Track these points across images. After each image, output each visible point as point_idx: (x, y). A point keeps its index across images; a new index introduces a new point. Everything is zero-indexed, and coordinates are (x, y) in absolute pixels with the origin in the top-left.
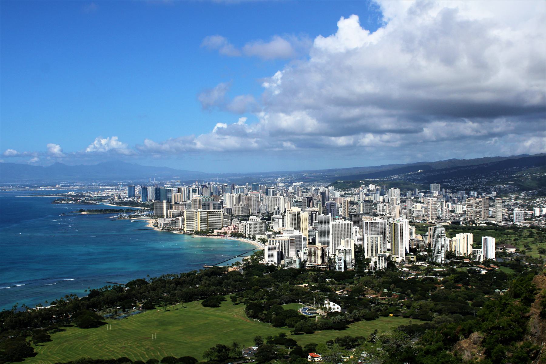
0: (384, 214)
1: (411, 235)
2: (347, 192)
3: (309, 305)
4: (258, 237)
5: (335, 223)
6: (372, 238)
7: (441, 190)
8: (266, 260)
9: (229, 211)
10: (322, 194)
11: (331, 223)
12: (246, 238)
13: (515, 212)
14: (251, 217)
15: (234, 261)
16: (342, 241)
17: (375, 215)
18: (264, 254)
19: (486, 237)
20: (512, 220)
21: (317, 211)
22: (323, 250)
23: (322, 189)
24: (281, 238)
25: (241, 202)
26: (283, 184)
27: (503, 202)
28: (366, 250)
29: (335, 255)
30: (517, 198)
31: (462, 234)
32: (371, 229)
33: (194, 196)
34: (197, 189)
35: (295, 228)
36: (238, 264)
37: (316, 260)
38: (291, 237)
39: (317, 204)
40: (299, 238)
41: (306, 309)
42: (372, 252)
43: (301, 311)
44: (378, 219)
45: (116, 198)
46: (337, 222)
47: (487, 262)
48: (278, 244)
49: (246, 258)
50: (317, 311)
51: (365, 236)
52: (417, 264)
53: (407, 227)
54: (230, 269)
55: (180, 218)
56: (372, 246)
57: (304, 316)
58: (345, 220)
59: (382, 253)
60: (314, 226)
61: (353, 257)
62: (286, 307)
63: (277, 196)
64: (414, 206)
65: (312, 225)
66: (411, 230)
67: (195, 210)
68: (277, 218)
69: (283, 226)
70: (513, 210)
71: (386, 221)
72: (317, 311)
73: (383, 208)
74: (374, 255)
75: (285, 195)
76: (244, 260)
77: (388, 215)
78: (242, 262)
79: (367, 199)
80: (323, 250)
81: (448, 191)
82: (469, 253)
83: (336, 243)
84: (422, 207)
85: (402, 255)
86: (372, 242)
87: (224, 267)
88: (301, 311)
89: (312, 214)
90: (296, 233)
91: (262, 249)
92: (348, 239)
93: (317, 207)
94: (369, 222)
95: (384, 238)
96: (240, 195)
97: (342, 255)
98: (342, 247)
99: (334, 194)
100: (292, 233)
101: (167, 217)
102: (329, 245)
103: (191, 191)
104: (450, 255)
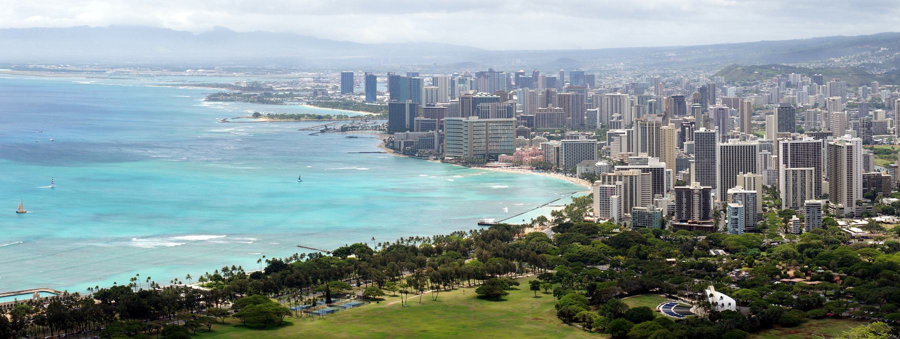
0: (817, 128)
1: (867, 167)
2: (748, 88)
3: (677, 299)
4: (580, 169)
5: (725, 144)
8: (594, 215)
11: (719, 144)
12: (558, 171)
16: (740, 176)
17: (802, 132)
18: (592, 202)
21: (691, 123)
22: (705, 194)
24: (625, 173)
25: (550, 105)
26: (629, 73)
28: (782, 196)
29: (725, 205)
32: (792, 156)
33: (463, 94)
34: (468, 78)
36: (542, 220)
37: (689, 215)
38: (644, 170)
39: (693, 109)
40: (658, 174)
41: (671, 305)
42: (794, 198)
43: (661, 309)
44: (806, 139)
45: (319, 92)
46: (731, 142)
48: (618, 183)
49: (559, 209)
50: (692, 310)
51: (782, 167)
52: (878, 219)
53: (860, 152)
54: (528, 231)
55: (435, 133)
57: (665, 318)
58: (744, 140)
59: (813, 201)
60: (685, 150)
62: (632, 303)
63: (619, 94)
64: (870, 113)
65: (682, 147)
66: (866, 158)
67: (464, 119)
68: (617, 134)
69: (629, 150)
71: (821, 140)
72: (692, 310)
73: (815, 119)
74: (799, 205)
75: (632, 91)
76: (553, 214)
78: (550, 218)
84: (887, 116)
85: (850, 204)
86: (795, 181)
87: (518, 227)
88: (661, 309)
89: (683, 128)
90: (654, 163)
92: (749, 174)
93: (693, 114)
94: (789, 143)
96: (548, 92)
98: (738, 189)
99: (725, 91)
100: (646, 162)
102: (714, 188)
103: (456, 84)
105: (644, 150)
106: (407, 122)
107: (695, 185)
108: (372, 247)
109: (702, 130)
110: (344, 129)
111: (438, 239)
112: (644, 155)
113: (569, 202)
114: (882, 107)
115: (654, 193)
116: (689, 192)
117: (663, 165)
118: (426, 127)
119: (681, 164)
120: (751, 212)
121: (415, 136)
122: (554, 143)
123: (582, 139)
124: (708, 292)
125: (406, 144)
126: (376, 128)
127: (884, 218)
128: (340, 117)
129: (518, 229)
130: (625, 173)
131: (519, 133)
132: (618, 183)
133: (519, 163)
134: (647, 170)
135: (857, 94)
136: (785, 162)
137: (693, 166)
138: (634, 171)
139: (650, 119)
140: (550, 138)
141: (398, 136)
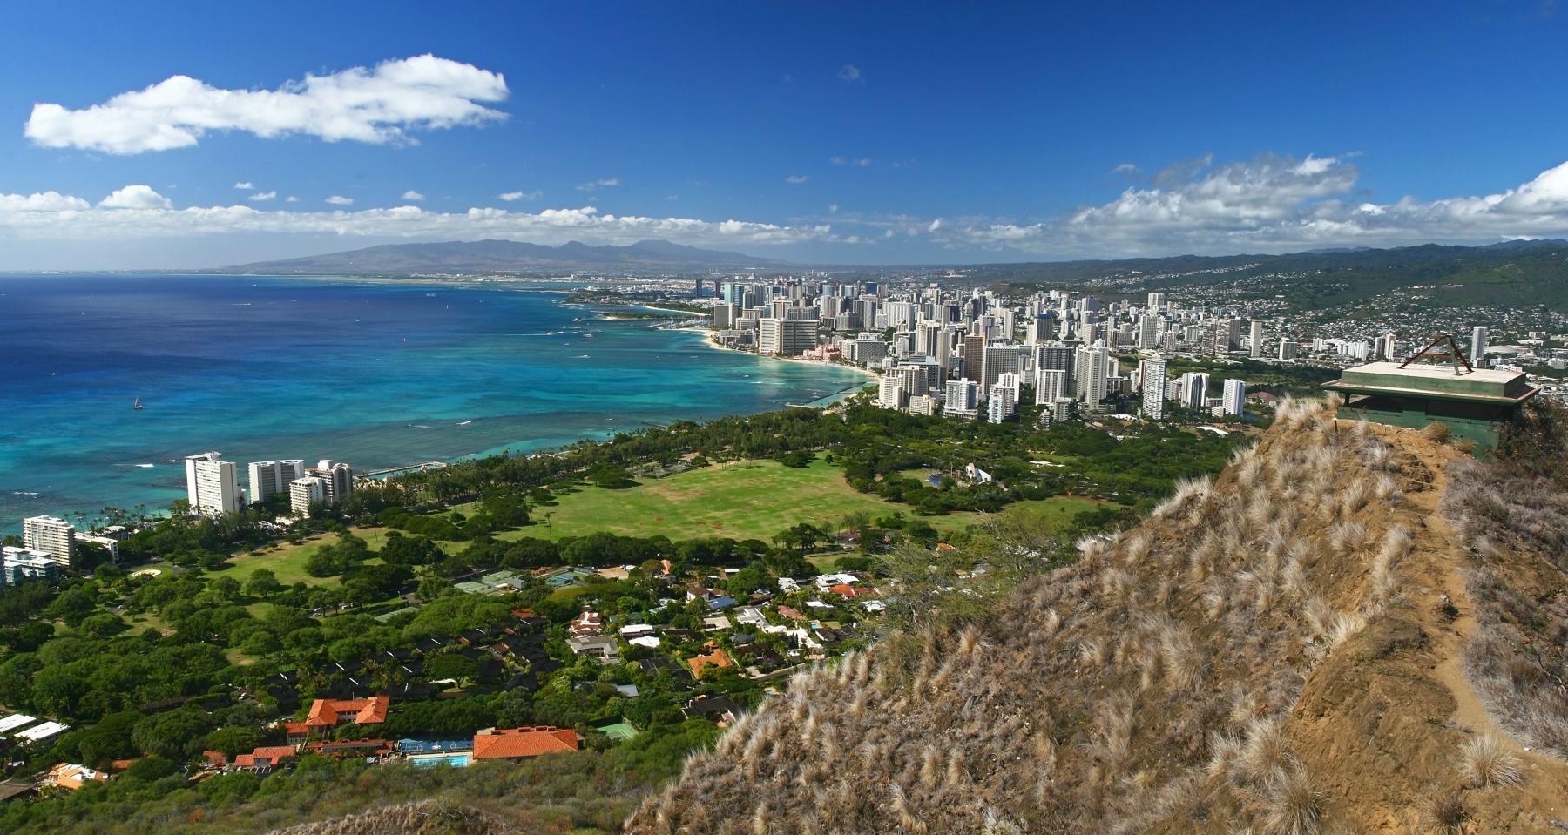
10: (975, 301)
11: (985, 348)
15: (831, 400)
16: (1001, 377)
23: (976, 295)
46: (996, 346)
47: (1227, 419)
54: (826, 412)
61: (1016, 399)
80: (971, 390)
83: (993, 379)
85: (1094, 401)
97: (1000, 398)
109: (972, 335)
123: (873, 338)
136: (1041, 365)
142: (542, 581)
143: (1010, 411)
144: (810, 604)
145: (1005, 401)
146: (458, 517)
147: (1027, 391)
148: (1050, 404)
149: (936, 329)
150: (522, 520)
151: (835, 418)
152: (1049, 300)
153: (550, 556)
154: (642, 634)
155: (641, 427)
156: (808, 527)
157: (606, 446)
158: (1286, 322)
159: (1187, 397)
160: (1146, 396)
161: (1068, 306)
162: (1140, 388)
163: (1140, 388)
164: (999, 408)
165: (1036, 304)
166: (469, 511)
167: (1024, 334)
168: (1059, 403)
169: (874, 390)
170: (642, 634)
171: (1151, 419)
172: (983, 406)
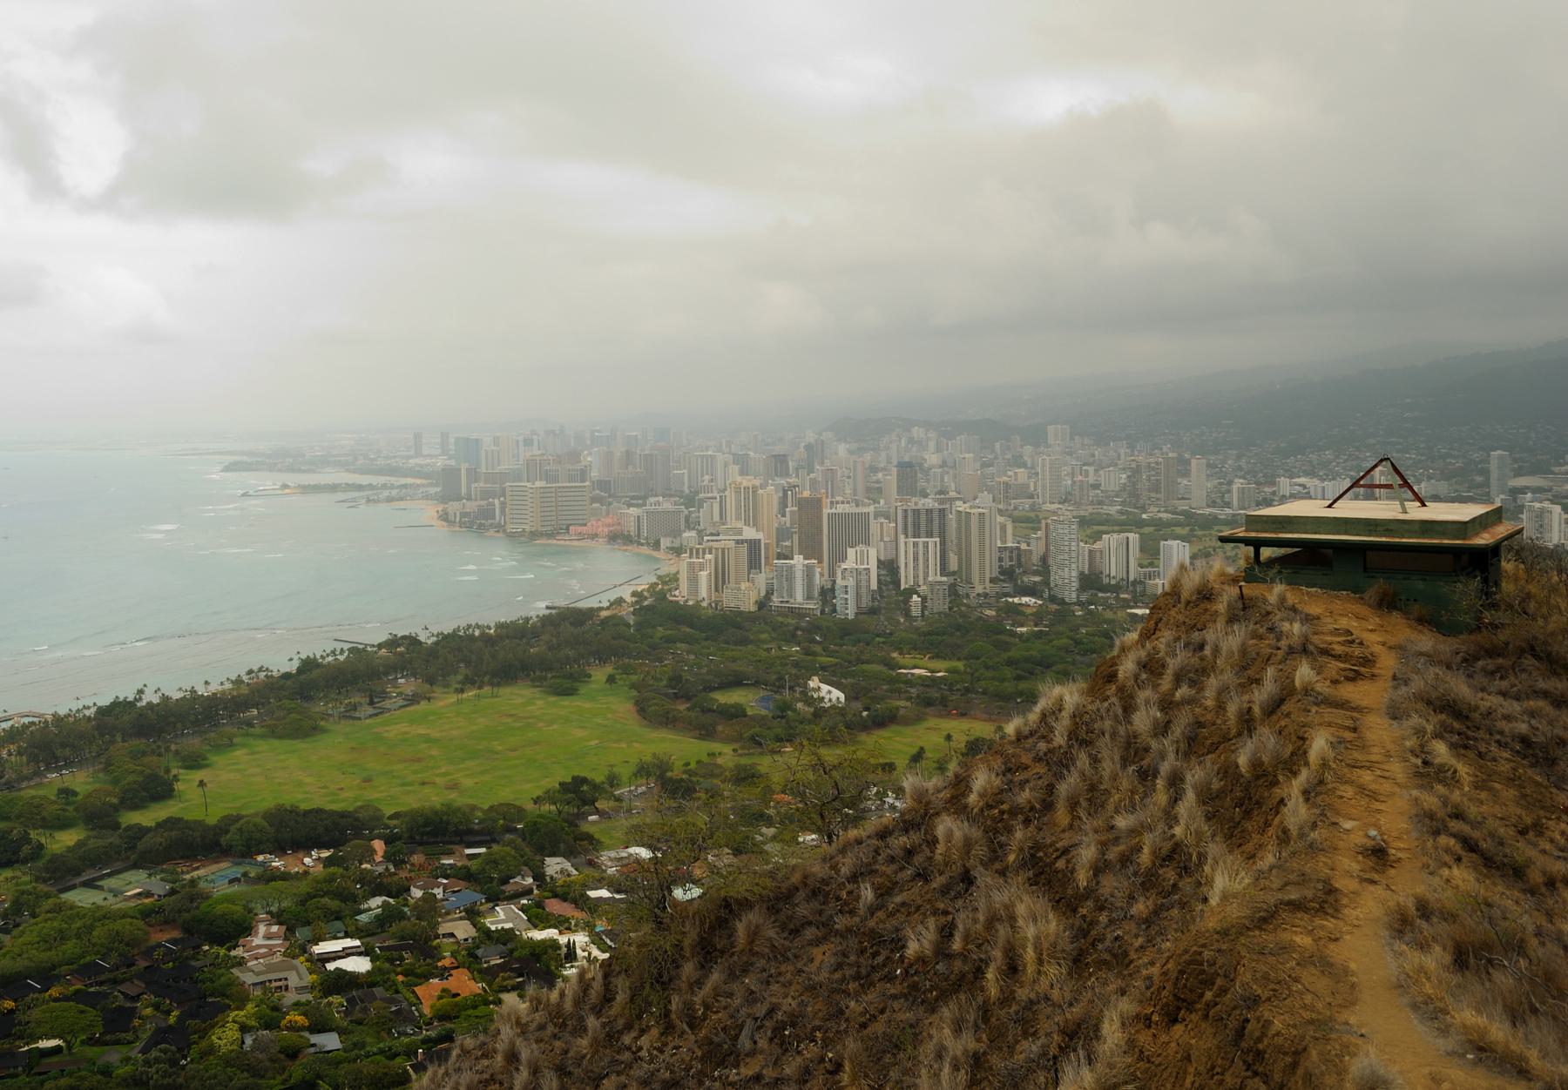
4: (665, 542)
6: (915, 545)
7: (1072, 439)
8: (681, 595)
9: (603, 485)
11: (826, 511)
13: (1235, 487)
14: (652, 500)
15: (613, 596)
16: (851, 552)
17: (926, 496)
19: (1170, 542)
20: (1228, 505)
24: (715, 545)
27: (1209, 466)
30: (1239, 457)
31: (1115, 536)
35: (747, 523)
36: (620, 601)
38: (738, 542)
40: (754, 546)
46: (840, 509)
48: (708, 556)
49: (639, 589)
51: (902, 538)
54: (604, 614)
56: (916, 568)
61: (874, 586)
70: (1230, 483)
77: (953, 494)
78: (629, 599)
79: (906, 459)
81: (1086, 441)
82: (1131, 578)
85: (982, 581)
87: (592, 609)
90: (750, 533)
91: (673, 570)
95: (943, 543)
97: (851, 582)
100: (740, 532)
101: (469, 499)
102: (820, 562)
104: (1091, 581)
105: (738, 518)
106: (464, 491)
107: (798, 561)
108: (422, 638)
109: (806, 494)
110: (389, 500)
111: (500, 626)
112: (740, 525)
113: (654, 580)
114: (1024, 465)
115: (750, 567)
116: (792, 567)
117: (760, 536)
118: (486, 495)
119: (782, 534)
120: (864, 590)
121: (471, 506)
122: (633, 511)
123: (667, 506)
124: (812, 684)
125: (463, 515)
126: (427, 497)
127: (1025, 600)
128: (384, 487)
129: (592, 612)
130: (715, 545)
131: (594, 500)
132: (708, 556)
133: (594, 536)
134: (742, 542)
135: (993, 451)
137: (796, 537)
138: (726, 541)
139: (745, 483)
140: (630, 505)
141: (454, 507)
142: (193, 882)
143: (866, 602)
144: (593, 894)
145: (858, 587)
146: (66, 793)
147: (889, 568)
148: (923, 589)
149: (755, 489)
150: (160, 790)
151: (613, 622)
152: (911, 441)
153: (206, 843)
154: (346, 953)
155: (339, 646)
156: (584, 780)
157: (287, 676)
158: (1239, 457)
159: (1113, 569)
160: (1053, 569)
161: (938, 449)
162: (1044, 559)
163: (1044, 559)
164: (851, 597)
165: (894, 447)
166: (81, 781)
167: (880, 490)
168: (932, 585)
169: (674, 578)
170: (346, 953)
171: (1062, 602)
172: (827, 594)
